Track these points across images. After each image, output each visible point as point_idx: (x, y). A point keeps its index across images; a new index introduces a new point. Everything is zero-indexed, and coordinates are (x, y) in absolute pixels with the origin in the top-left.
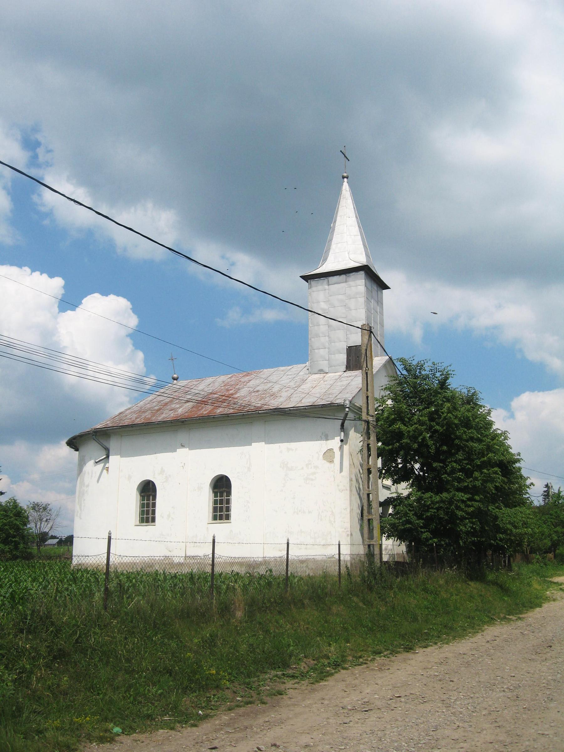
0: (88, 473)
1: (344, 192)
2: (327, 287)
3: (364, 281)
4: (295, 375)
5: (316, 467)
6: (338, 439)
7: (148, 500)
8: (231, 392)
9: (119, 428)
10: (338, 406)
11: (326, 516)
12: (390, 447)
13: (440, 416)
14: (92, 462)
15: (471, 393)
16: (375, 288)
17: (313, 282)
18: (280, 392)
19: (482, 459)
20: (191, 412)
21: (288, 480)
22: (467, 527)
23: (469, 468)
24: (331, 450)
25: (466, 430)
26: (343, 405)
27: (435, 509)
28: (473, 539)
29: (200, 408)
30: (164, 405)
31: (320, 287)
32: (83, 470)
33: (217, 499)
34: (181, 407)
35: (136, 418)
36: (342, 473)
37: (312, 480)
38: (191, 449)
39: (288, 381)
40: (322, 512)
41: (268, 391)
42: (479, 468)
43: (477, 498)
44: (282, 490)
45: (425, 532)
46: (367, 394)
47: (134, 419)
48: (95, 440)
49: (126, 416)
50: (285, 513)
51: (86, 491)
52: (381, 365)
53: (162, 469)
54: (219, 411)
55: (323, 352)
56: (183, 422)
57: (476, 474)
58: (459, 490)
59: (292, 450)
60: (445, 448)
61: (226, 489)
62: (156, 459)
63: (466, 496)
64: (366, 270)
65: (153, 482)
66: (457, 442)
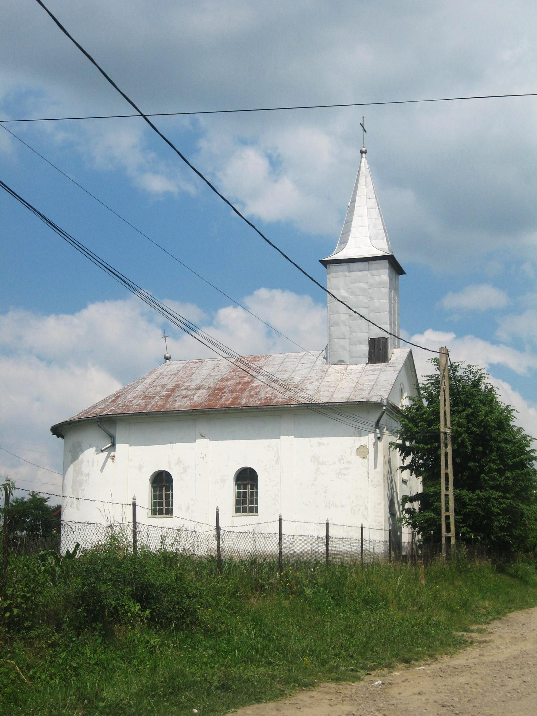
0: (88, 462)
1: (363, 169)
2: (347, 274)
3: (388, 270)
4: (313, 364)
5: (349, 462)
6: (372, 436)
7: (161, 491)
8: (246, 379)
9: (132, 416)
10: (375, 403)
11: (359, 510)
12: (429, 446)
13: (476, 419)
14: (94, 449)
15: (488, 388)
16: (394, 275)
17: (333, 267)
18: (304, 384)
19: (515, 460)
20: (209, 400)
21: (319, 474)
22: (501, 523)
23: (501, 468)
24: (364, 446)
25: (501, 432)
26: (381, 403)
27: (472, 506)
28: (503, 533)
29: (218, 397)
30: (172, 391)
31: (340, 274)
32: (80, 458)
33: (241, 492)
34: (194, 394)
35: (146, 405)
36: (376, 470)
37: (345, 475)
38: (211, 440)
39: (307, 370)
40: (355, 506)
41: (289, 381)
42: (512, 468)
43: (508, 495)
44: (313, 485)
45: (463, 527)
46: (445, 409)
47: (144, 406)
48: (101, 427)
49: (131, 401)
50: (317, 506)
51: (86, 481)
52: (405, 359)
53: (179, 459)
54: (243, 402)
55: (344, 342)
56: (203, 412)
57: (508, 474)
58: (492, 488)
59: (324, 445)
60: (481, 448)
61: (250, 482)
62: (172, 448)
63: (497, 493)
64: (391, 260)
65: (166, 472)
66: (492, 443)
